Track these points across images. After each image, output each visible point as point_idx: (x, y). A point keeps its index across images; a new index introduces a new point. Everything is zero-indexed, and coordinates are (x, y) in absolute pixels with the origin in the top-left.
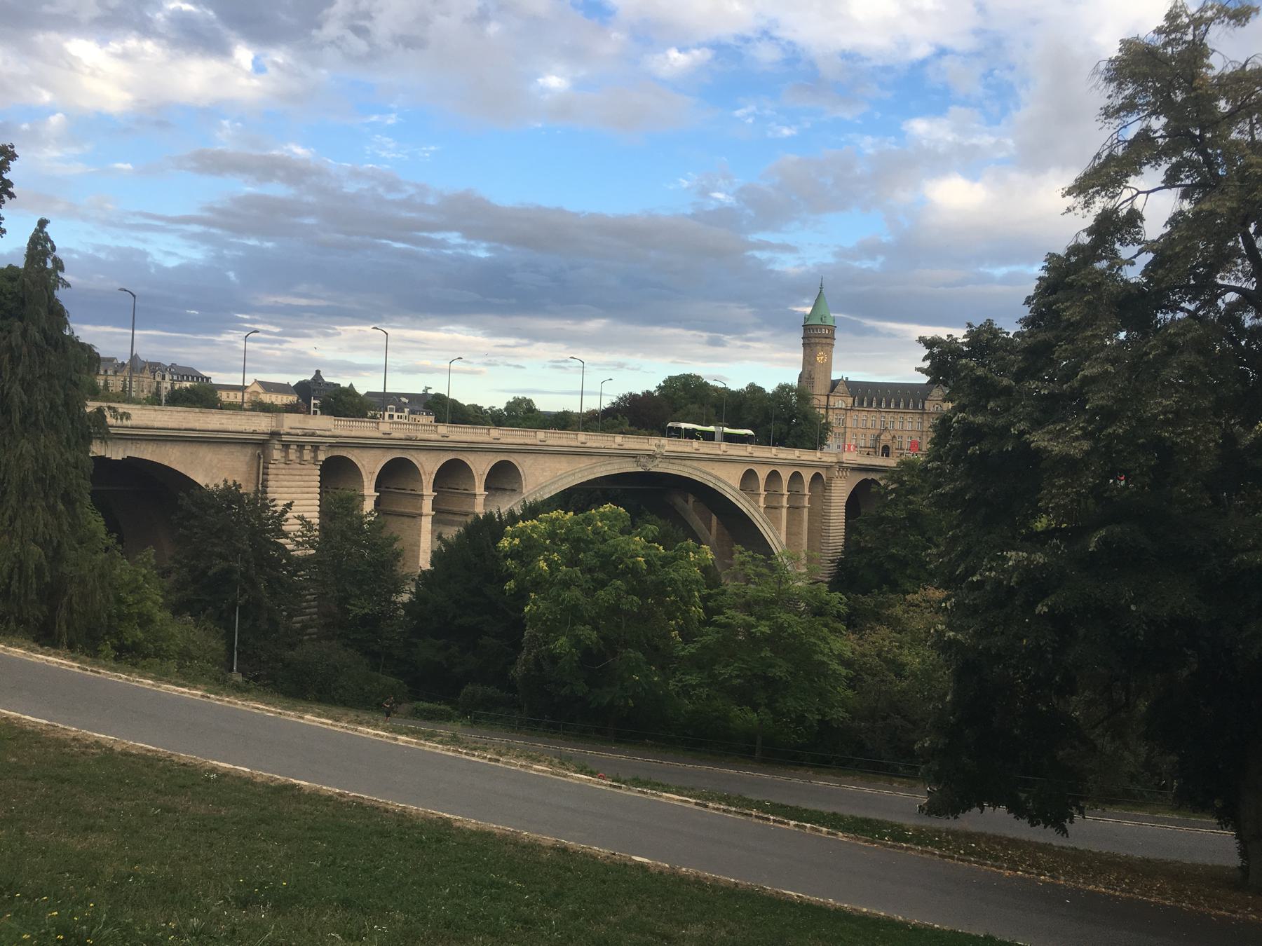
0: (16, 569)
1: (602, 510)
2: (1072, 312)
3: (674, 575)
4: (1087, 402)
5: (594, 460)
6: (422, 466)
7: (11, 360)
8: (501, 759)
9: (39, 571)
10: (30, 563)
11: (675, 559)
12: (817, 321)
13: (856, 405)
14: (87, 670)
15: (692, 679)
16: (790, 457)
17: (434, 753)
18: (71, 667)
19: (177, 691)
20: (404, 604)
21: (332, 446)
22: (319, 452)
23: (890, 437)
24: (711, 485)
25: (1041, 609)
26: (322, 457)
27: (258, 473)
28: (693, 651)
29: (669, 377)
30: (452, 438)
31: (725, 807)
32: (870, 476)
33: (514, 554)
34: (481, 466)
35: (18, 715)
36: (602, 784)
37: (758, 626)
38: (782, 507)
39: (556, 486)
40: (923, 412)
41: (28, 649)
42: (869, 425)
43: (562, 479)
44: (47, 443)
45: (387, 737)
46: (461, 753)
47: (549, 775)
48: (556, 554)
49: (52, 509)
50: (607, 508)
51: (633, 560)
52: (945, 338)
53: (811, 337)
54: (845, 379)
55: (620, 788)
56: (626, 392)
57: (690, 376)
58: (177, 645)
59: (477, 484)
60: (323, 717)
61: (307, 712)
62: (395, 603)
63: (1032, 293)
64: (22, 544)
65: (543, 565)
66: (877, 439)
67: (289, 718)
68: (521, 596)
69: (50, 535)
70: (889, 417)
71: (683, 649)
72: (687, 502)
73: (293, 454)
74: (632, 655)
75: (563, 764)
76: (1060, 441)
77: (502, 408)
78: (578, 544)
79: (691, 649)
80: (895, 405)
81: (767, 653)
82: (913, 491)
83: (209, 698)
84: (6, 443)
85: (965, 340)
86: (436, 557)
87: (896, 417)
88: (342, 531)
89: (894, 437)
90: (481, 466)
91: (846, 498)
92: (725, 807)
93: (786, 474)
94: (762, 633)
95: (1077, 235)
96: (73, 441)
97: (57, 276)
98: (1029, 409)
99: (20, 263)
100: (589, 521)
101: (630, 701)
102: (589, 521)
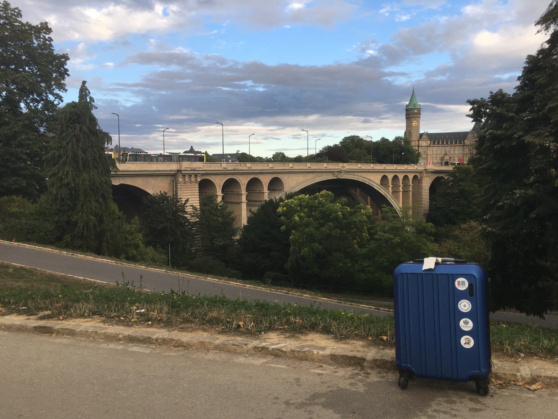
0: (85, 226)
1: (321, 193)
2: (541, 79)
3: (355, 219)
4: (551, 119)
5: (315, 175)
6: (241, 181)
7: (77, 140)
8: (290, 293)
9: (94, 226)
10: (91, 223)
11: (355, 212)
12: (412, 107)
13: (432, 144)
14: (118, 264)
15: (366, 264)
16: (402, 169)
17: (262, 291)
18: (111, 262)
19: (155, 270)
20: (237, 240)
21: (203, 175)
22: (198, 178)
23: (448, 158)
24: (367, 183)
25: (533, 215)
26: (199, 180)
27: (174, 188)
28: (366, 251)
29: (345, 137)
30: (253, 168)
31: (388, 310)
32: (440, 175)
33: (284, 214)
34: (266, 180)
35: (95, 280)
36: (333, 302)
37: (394, 239)
38: (400, 191)
39: (299, 187)
40: (464, 145)
41: (94, 257)
42: (438, 152)
43: (301, 184)
44: (94, 174)
45: (241, 285)
46: (273, 291)
47: (310, 299)
48: (302, 213)
49: (97, 201)
50: (323, 192)
51: (336, 214)
52: (480, 100)
54: (426, 132)
55: (341, 303)
56: (326, 146)
57: (354, 136)
58: (150, 256)
59: (264, 188)
60: (214, 278)
61: (208, 277)
62: (233, 239)
63: (520, 74)
64: (87, 215)
65: (297, 218)
66: (442, 159)
67: (201, 279)
68: (287, 233)
69: (98, 212)
70: (448, 149)
71: (361, 251)
72: (356, 191)
73: (187, 179)
74: (338, 255)
75: (316, 294)
76: (539, 138)
77: (271, 157)
78: (312, 208)
79: (364, 250)
81: (399, 250)
82: (461, 180)
83: (167, 272)
84: (77, 175)
85: (489, 100)
86: (249, 219)
87: (451, 148)
88: (210, 210)
89: (450, 157)
90: (266, 180)
91: (429, 186)
92: (388, 310)
93: (401, 177)
94: (397, 242)
95: (542, 45)
96: (104, 172)
97: (92, 104)
98: (523, 126)
99: (77, 100)
100: (316, 198)
101: (338, 275)
102: (316, 198)
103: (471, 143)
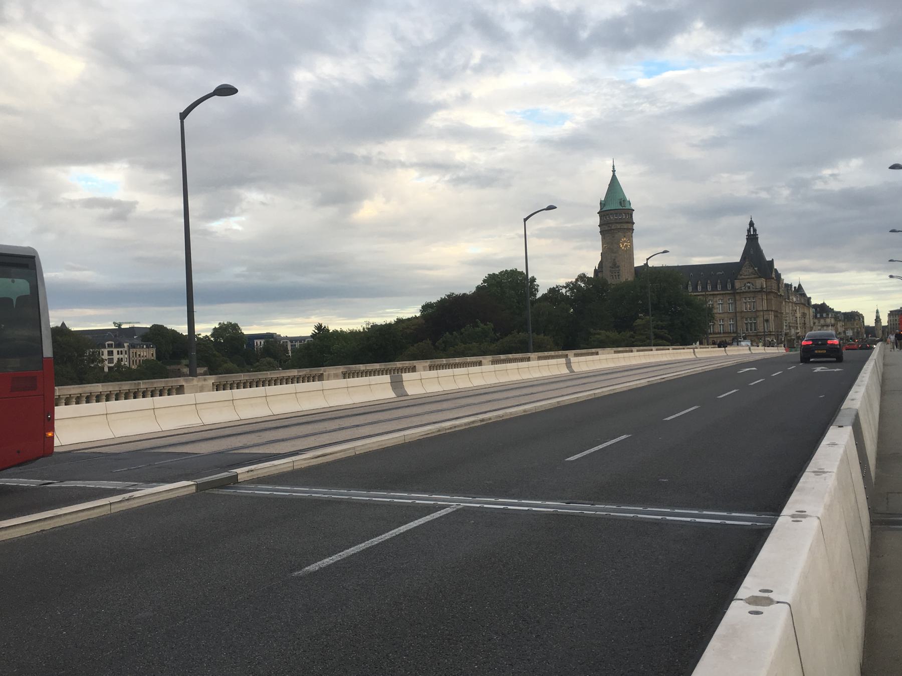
77: (209, 334)
80: (702, 288)
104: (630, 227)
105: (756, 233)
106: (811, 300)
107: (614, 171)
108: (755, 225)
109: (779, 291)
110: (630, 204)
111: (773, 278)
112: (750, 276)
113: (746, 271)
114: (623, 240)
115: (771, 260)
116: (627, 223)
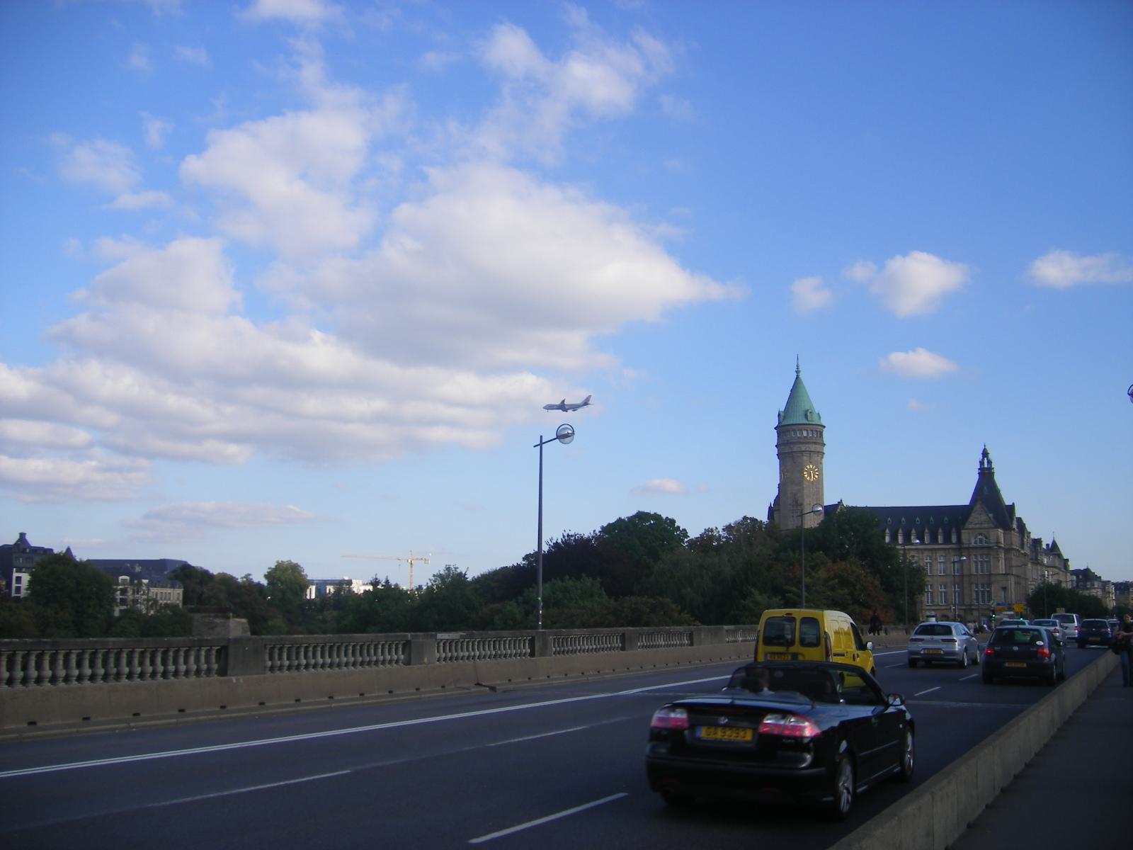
53: (791, 443)
103: (981, 540)
104: (818, 450)
105: (991, 466)
106: (1069, 563)
107: (798, 372)
108: (990, 456)
109: (1023, 548)
110: (820, 418)
111: (1014, 529)
112: (983, 526)
113: (980, 518)
114: (808, 467)
115: (1011, 504)
116: (815, 443)
